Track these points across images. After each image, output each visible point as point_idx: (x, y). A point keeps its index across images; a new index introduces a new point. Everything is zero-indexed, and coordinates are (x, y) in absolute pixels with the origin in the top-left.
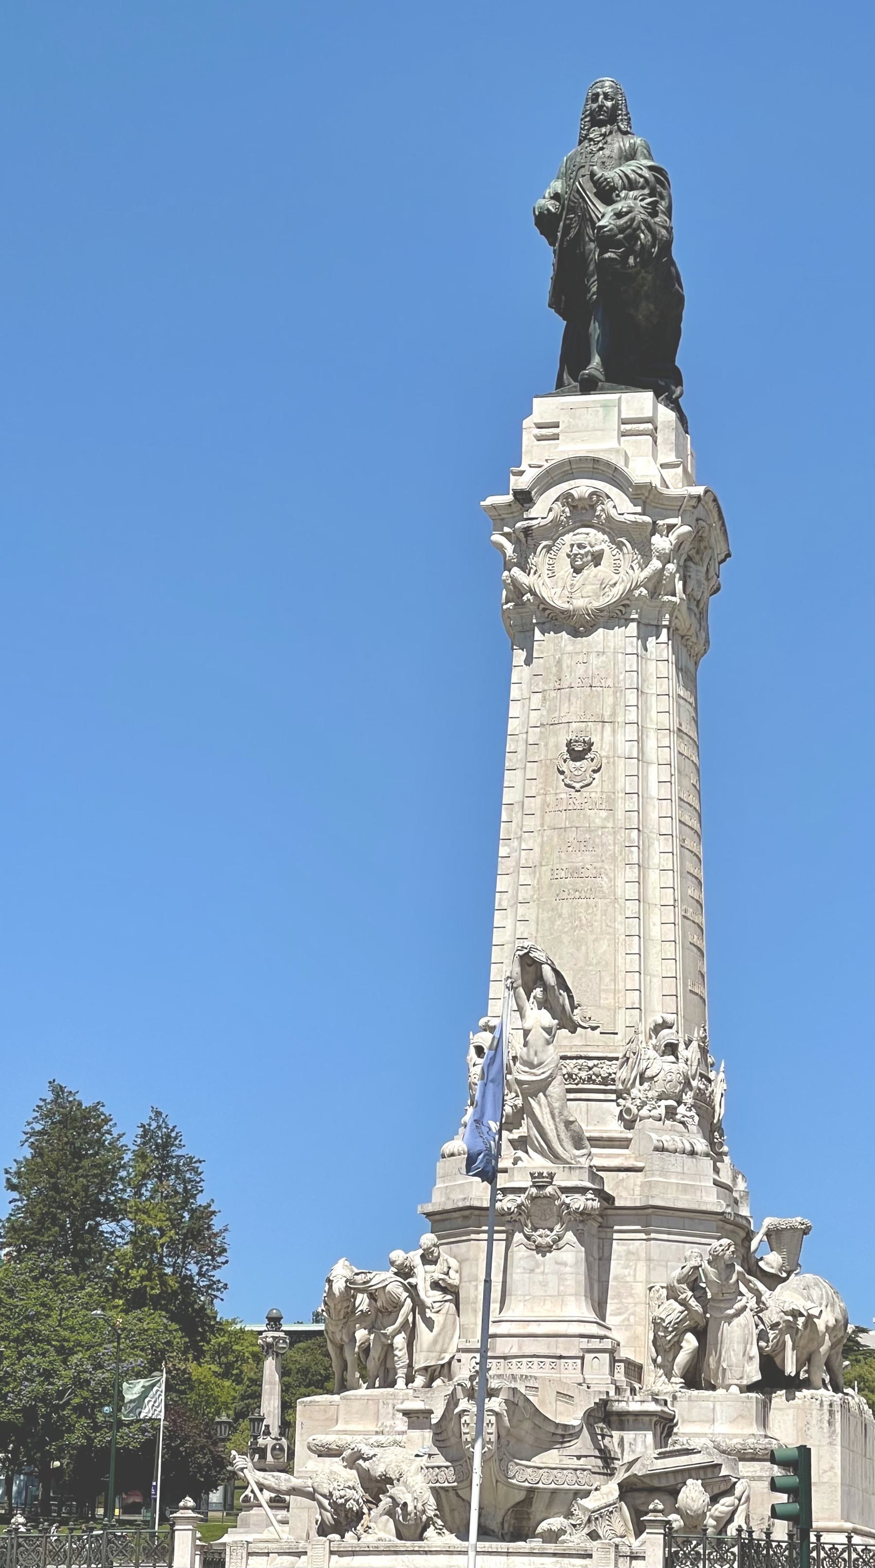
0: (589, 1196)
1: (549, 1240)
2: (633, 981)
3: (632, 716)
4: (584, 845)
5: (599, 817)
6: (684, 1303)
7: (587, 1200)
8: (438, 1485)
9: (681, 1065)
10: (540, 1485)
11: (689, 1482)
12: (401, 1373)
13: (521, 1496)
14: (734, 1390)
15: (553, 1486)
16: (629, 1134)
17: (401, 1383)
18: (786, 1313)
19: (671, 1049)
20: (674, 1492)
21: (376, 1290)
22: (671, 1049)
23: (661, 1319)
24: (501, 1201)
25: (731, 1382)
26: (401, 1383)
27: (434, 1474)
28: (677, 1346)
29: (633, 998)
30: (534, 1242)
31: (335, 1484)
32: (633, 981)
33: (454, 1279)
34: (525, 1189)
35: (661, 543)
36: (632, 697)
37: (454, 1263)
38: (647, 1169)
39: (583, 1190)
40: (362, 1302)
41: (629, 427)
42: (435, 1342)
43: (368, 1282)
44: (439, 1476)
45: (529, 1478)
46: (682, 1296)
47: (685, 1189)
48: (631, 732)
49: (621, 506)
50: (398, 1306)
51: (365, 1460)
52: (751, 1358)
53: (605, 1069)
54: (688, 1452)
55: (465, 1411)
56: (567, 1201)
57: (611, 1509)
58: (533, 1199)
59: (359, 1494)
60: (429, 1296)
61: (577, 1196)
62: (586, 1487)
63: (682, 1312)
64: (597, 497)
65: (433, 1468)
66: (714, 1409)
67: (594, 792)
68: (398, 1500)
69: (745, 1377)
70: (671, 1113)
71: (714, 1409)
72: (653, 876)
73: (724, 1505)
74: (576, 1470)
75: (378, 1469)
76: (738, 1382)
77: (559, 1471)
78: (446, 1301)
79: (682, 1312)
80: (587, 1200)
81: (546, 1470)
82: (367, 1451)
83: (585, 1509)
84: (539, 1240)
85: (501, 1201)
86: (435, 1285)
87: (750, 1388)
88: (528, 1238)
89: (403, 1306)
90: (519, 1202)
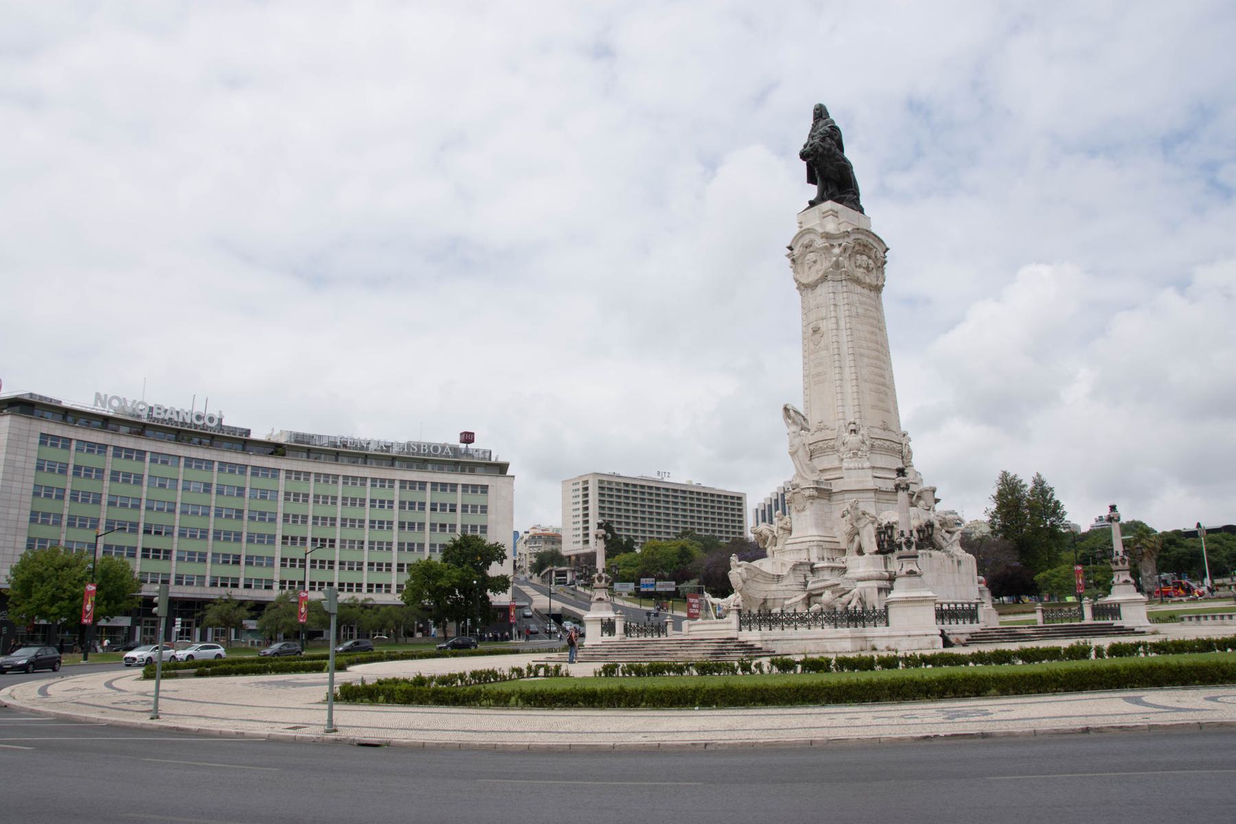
2: (840, 409)
3: (833, 314)
4: (821, 364)
5: (824, 353)
9: (859, 437)
19: (854, 431)
20: (821, 595)
22: (854, 431)
28: (852, 541)
29: (840, 416)
32: (840, 409)
35: (837, 251)
36: (832, 308)
41: (825, 215)
47: (859, 482)
48: (833, 320)
49: (820, 243)
53: (832, 443)
64: (812, 241)
67: (822, 345)
70: (855, 454)
72: (847, 371)
73: (845, 598)
87: (877, 553)
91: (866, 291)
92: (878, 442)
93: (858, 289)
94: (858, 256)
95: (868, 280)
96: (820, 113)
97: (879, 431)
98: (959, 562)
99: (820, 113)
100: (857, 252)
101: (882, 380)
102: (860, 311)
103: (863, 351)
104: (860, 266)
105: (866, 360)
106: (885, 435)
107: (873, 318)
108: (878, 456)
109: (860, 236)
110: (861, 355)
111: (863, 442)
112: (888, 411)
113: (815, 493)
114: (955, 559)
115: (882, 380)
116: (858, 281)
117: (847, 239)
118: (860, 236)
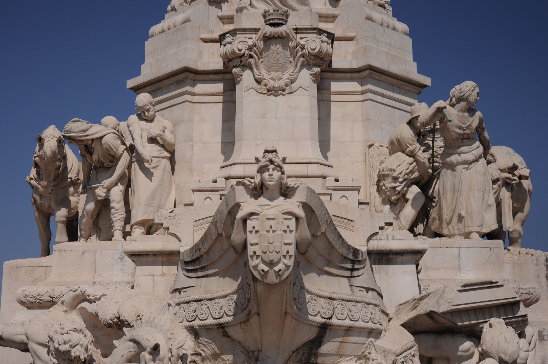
0: (324, 38)
1: (281, 83)
6: (412, 155)
7: (322, 42)
8: (197, 323)
10: (334, 321)
11: (493, 320)
12: (118, 224)
13: (312, 334)
14: (475, 236)
15: (348, 322)
16: (335, 11)
17: (118, 234)
18: (501, 171)
21: (93, 140)
23: (391, 170)
24: (230, 43)
25: (471, 229)
26: (118, 234)
27: (192, 309)
30: (266, 85)
31: (57, 327)
33: (169, 136)
34: (256, 31)
37: (167, 123)
38: (359, 37)
39: (320, 32)
40: (74, 164)
42: (153, 197)
43: (85, 131)
44: (198, 312)
45: (322, 311)
46: (411, 148)
50: (114, 159)
51: (90, 302)
52: (489, 206)
54: (491, 285)
55: (252, 214)
56: (302, 42)
57: (412, 351)
58: (268, 39)
59: (87, 338)
60: (148, 151)
61: (312, 36)
62: (377, 326)
63: (411, 164)
65: (188, 303)
66: (459, 255)
68: (144, 343)
69: (484, 226)
71: (459, 255)
74: (368, 304)
75: (107, 311)
76: (478, 229)
77: (353, 304)
78: (163, 158)
79: (411, 164)
80: (322, 42)
81: (340, 302)
82: (91, 291)
83: (385, 352)
84: (271, 84)
85: (230, 43)
86: (152, 140)
88: (259, 82)
89: (120, 158)
90: (250, 43)
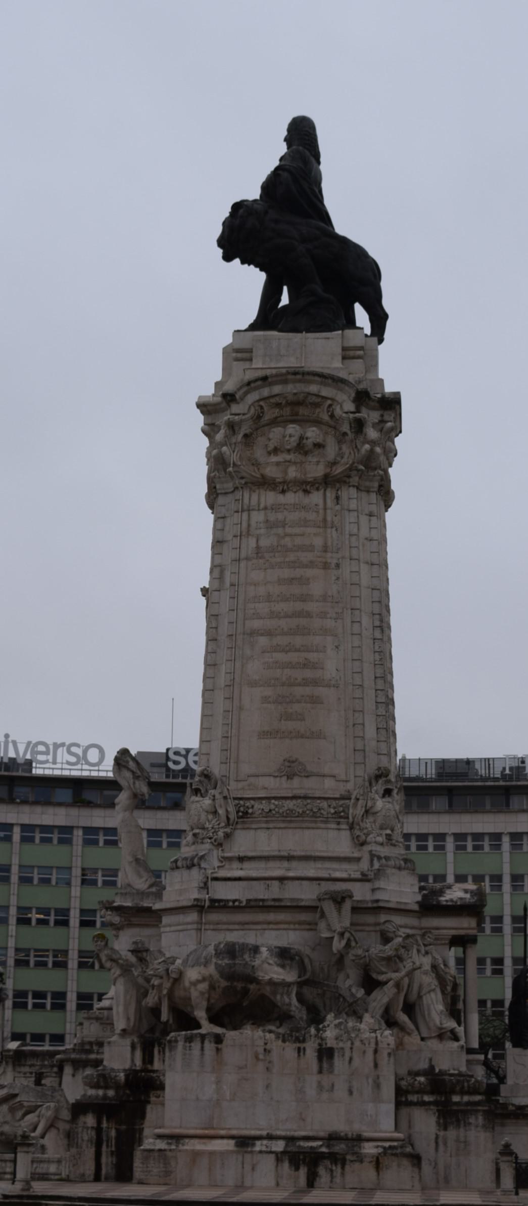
9: (207, 802)
91: (291, 498)
92: (264, 806)
93: (270, 497)
94: (276, 433)
95: (293, 473)
96: (302, 135)
97: (271, 782)
98: (326, 1054)
99: (302, 135)
100: (274, 422)
101: (308, 674)
102: (264, 543)
103: (256, 624)
104: (276, 451)
105: (263, 641)
106: (297, 786)
107: (310, 548)
108: (262, 835)
109: (277, 389)
110: (253, 633)
111: (215, 812)
112: (319, 735)
113: (116, 919)
114: (311, 1048)
115: (308, 674)
116: (265, 483)
117: (235, 408)
118: (277, 389)
